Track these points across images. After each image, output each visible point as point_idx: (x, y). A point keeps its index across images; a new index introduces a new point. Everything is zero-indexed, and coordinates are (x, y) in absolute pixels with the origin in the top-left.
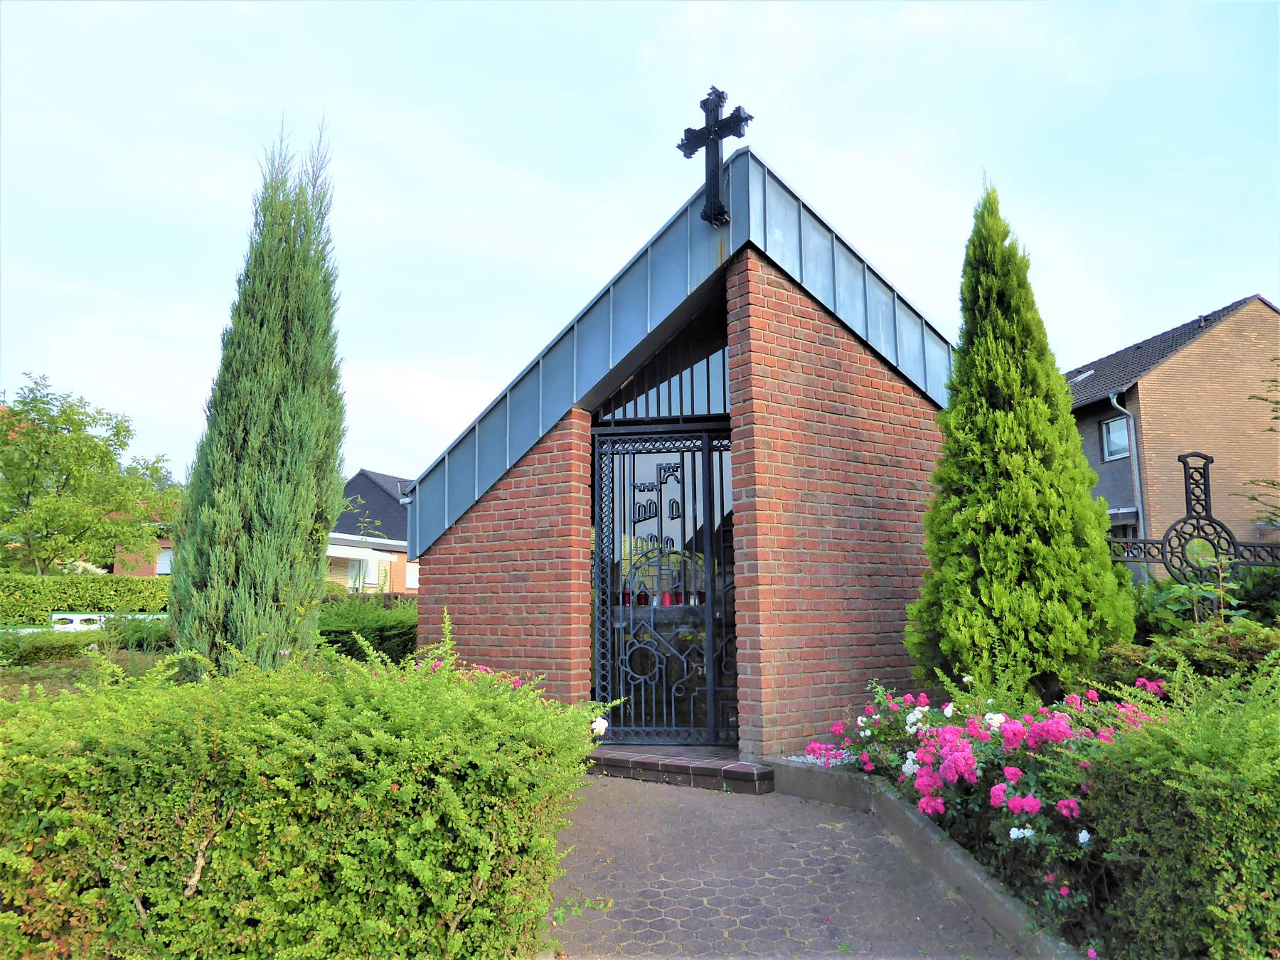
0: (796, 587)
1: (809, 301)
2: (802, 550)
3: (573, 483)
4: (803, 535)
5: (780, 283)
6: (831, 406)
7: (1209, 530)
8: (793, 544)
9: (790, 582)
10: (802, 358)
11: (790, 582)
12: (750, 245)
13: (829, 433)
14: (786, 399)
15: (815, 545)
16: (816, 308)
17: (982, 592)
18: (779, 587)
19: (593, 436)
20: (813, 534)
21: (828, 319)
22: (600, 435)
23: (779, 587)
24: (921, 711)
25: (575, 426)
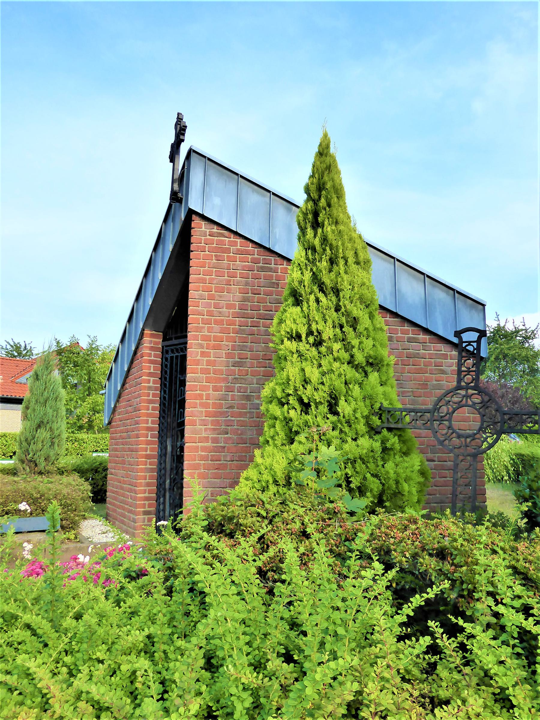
0: (222, 445)
1: (248, 242)
2: (229, 418)
3: (143, 377)
4: (231, 407)
5: (220, 233)
6: (266, 314)
7: (444, 409)
8: (222, 414)
9: (215, 440)
10: (238, 283)
11: (215, 440)
12: (191, 213)
13: (263, 334)
14: (220, 313)
15: (241, 415)
16: (254, 246)
17: (42, 488)
18: (206, 444)
19: (163, 347)
20: (244, 407)
21: (267, 253)
22: (166, 346)
23: (206, 444)
24: (527, 506)
25: (146, 342)
